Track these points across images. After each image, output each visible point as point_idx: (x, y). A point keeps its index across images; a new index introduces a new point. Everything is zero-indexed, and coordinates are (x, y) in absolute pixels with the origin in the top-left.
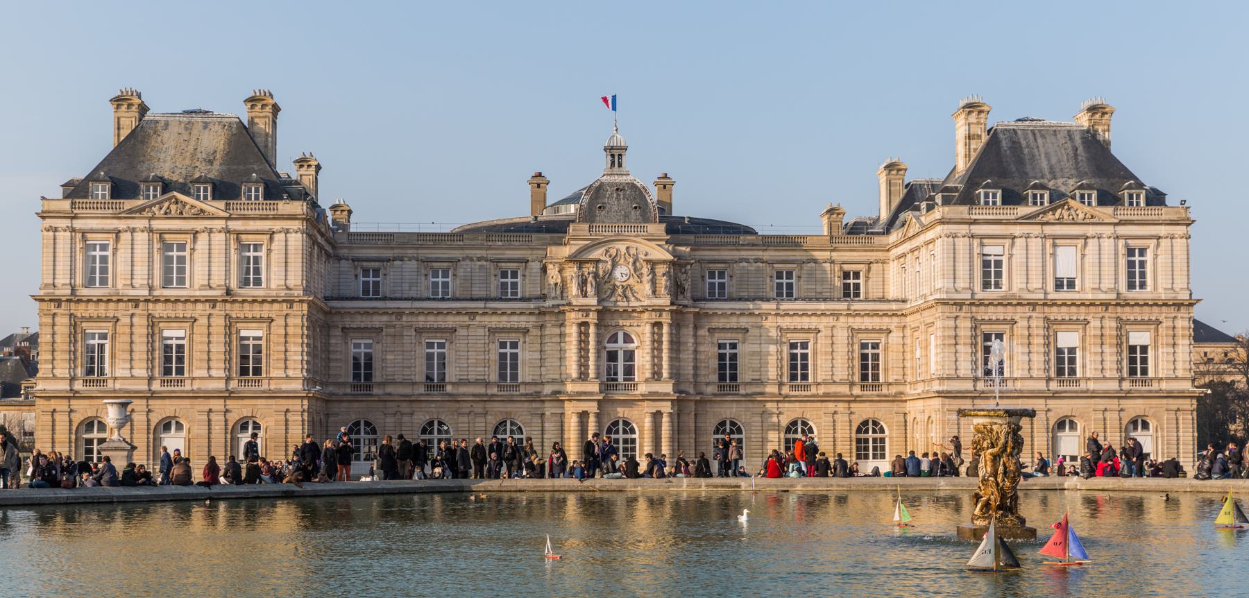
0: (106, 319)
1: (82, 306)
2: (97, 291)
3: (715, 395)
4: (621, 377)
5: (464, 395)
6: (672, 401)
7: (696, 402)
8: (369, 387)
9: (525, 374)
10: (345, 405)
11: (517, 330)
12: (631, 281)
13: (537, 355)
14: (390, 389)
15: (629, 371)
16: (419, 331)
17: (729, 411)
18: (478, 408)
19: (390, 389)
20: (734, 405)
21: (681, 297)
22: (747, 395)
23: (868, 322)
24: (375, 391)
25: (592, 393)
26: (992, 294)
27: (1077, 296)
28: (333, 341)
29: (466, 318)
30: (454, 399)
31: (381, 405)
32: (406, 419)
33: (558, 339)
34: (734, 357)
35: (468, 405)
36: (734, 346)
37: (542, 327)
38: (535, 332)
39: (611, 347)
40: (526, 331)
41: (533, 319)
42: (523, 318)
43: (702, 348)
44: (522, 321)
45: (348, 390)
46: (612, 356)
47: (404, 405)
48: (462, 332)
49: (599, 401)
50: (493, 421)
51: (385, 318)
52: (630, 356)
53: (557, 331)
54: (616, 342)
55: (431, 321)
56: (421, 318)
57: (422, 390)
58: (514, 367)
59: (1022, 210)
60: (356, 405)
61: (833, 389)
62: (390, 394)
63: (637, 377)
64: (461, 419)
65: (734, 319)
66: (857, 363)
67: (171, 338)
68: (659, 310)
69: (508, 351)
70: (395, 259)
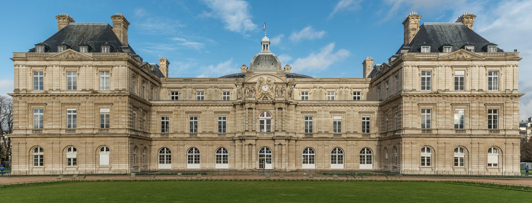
0: (42, 104)
1: (31, 98)
2: (39, 91)
3: (303, 138)
4: (265, 130)
5: (204, 138)
6: (286, 140)
7: (296, 140)
8: (168, 134)
9: (228, 130)
10: (158, 142)
11: (225, 112)
12: (269, 91)
13: (233, 122)
14: (176, 135)
15: (269, 127)
16: (187, 113)
17: (309, 144)
18: (210, 143)
19: (176, 135)
20: (311, 142)
21: (290, 98)
22: (316, 138)
23: (365, 109)
24: (170, 136)
25: (253, 136)
26: (426, 91)
27: (465, 93)
28: (153, 117)
29: (205, 107)
30: (200, 139)
31: (172, 142)
32: (182, 147)
33: (240, 115)
34: (311, 123)
35: (206, 142)
36: (311, 118)
37: (235, 111)
38: (232, 113)
39: (261, 118)
40: (229, 112)
41: (231, 107)
42: (228, 107)
43: (298, 119)
44: (227, 109)
45: (159, 136)
46: (262, 122)
47: (181, 141)
48: (203, 113)
49: (256, 140)
50: (216, 148)
51: (174, 108)
52: (269, 121)
53: (240, 112)
54: (263, 116)
55: (191, 109)
56: (188, 107)
57: (188, 136)
58: (224, 127)
59: (441, 54)
60: (162, 142)
61: (351, 136)
62: (175, 138)
63: (272, 130)
64: (203, 147)
65: (311, 107)
66: (360, 126)
67: (70, 112)
68: (281, 102)
69: (222, 120)
70: (183, 87)
